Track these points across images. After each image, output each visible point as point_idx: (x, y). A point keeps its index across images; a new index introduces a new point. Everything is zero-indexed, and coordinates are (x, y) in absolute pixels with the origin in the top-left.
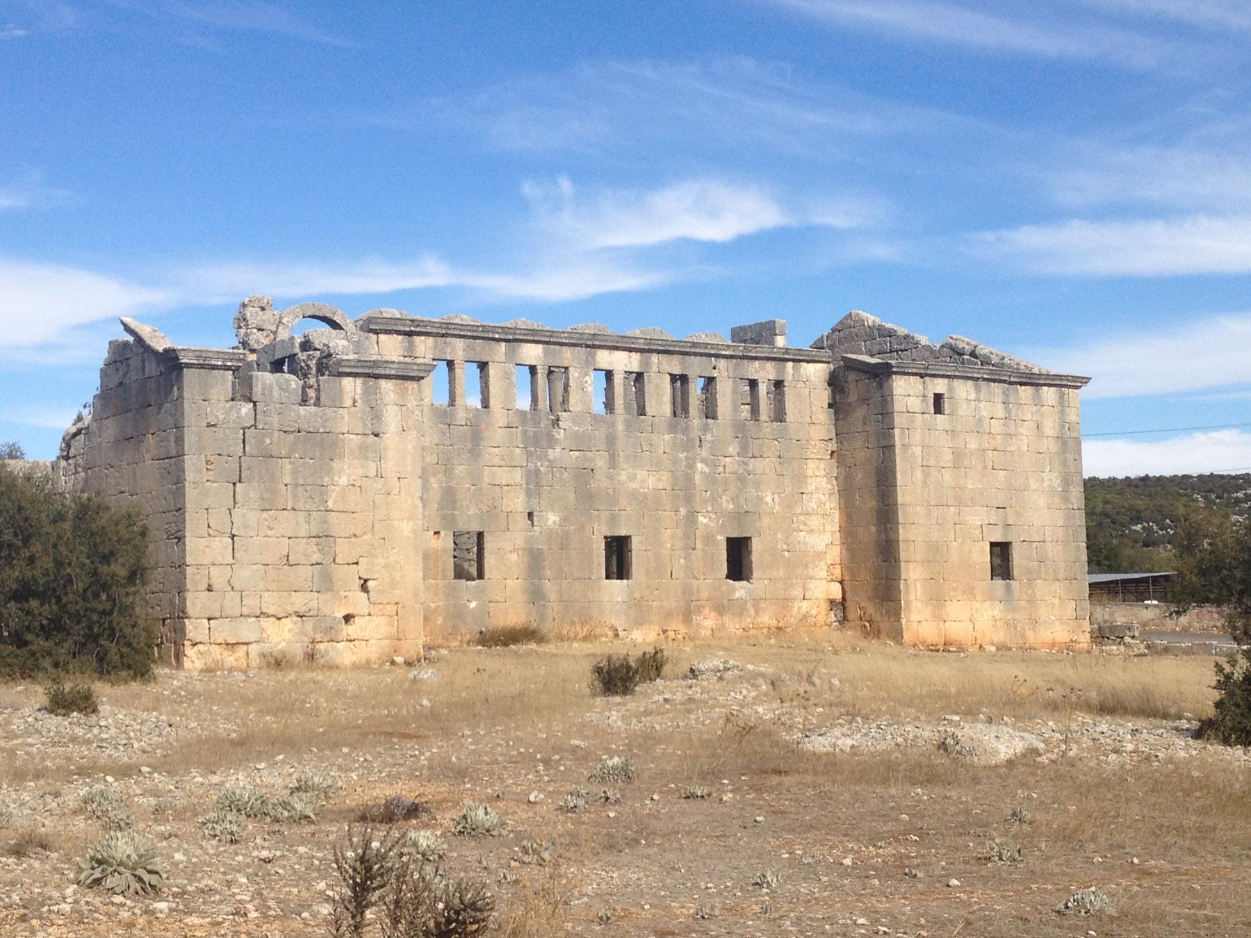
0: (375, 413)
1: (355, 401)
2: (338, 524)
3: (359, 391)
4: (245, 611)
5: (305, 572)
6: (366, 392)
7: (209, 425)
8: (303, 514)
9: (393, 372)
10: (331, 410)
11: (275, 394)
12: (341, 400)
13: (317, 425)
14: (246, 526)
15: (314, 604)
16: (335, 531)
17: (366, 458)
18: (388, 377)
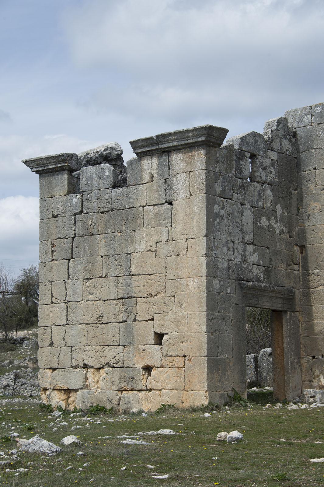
0: (168, 184)
1: (152, 177)
2: (138, 286)
3: (155, 166)
4: (74, 363)
5: (114, 328)
6: (160, 166)
7: (54, 216)
8: (113, 279)
9: (175, 143)
10: (134, 187)
11: (95, 183)
12: (141, 177)
13: (124, 203)
14: (75, 294)
15: (120, 357)
16: (135, 292)
17: (160, 225)
18: (177, 149)
